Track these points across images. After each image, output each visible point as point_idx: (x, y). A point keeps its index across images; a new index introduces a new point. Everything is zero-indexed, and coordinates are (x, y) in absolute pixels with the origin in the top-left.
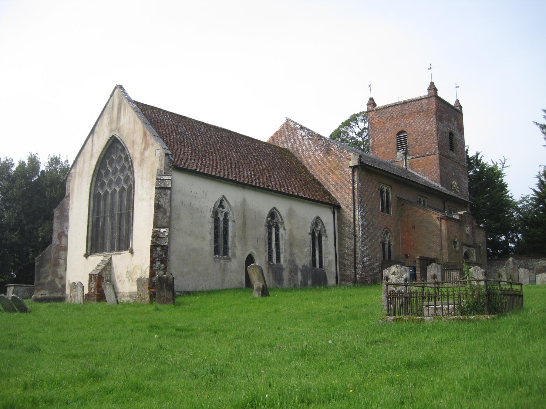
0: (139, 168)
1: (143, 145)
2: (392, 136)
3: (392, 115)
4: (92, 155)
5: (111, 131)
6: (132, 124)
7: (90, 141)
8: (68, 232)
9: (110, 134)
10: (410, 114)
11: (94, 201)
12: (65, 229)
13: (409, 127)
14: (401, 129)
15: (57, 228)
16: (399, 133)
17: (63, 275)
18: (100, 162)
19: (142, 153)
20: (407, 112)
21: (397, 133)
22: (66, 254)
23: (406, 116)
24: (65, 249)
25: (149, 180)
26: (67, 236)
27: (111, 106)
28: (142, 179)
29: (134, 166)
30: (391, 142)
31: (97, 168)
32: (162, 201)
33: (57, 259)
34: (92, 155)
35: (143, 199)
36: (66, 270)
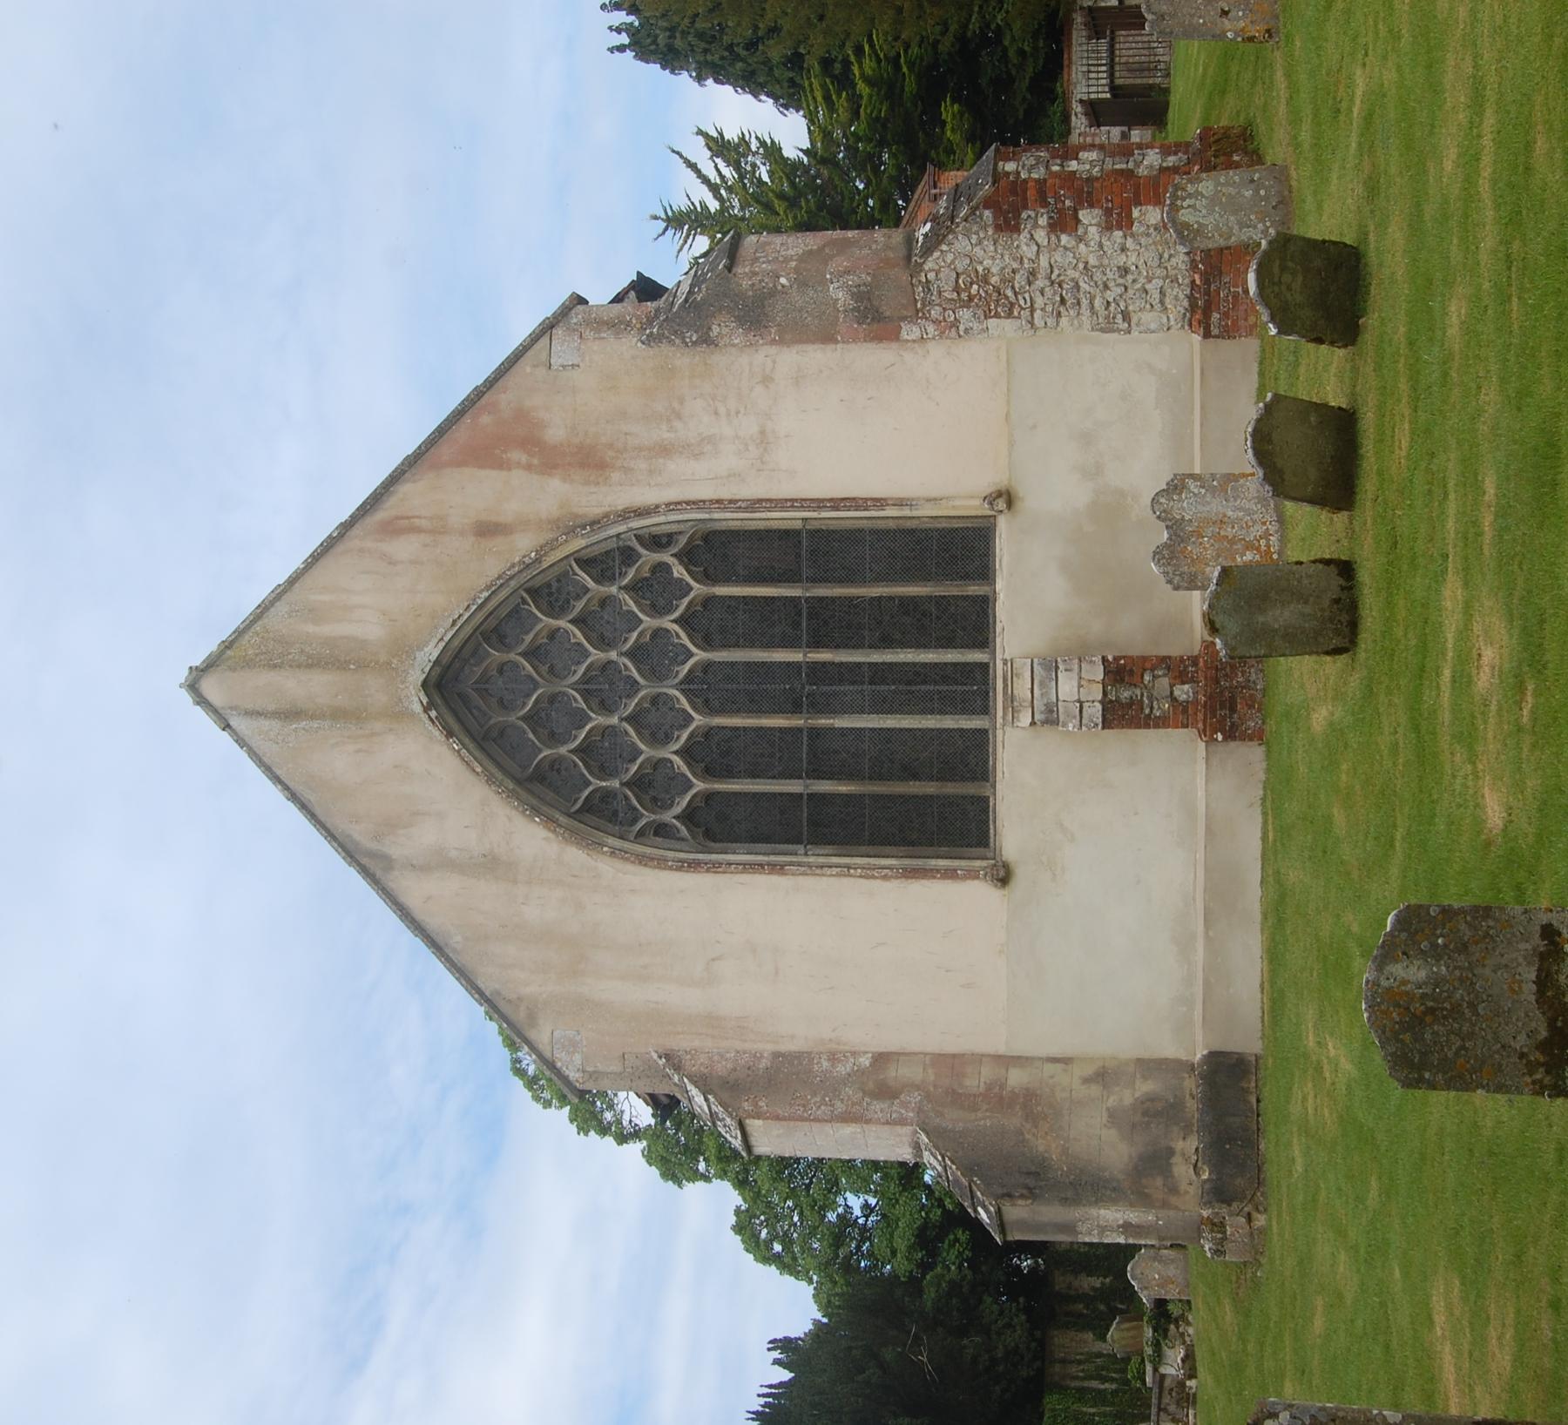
0: (616, 476)
1: (517, 455)
4: (491, 865)
5: (398, 714)
6: (404, 548)
7: (414, 890)
8: (854, 1054)
9: (413, 715)
11: (726, 853)
12: (842, 1069)
15: (838, 1104)
17: (1089, 1070)
18: (534, 802)
19: (550, 460)
22: (978, 1059)
24: (951, 1063)
25: (682, 401)
26: (881, 1059)
27: (273, 725)
28: (664, 450)
29: (596, 511)
31: (563, 819)
32: (791, 252)
33: (998, 1098)
34: (491, 865)
35: (763, 433)
36: (1065, 1061)
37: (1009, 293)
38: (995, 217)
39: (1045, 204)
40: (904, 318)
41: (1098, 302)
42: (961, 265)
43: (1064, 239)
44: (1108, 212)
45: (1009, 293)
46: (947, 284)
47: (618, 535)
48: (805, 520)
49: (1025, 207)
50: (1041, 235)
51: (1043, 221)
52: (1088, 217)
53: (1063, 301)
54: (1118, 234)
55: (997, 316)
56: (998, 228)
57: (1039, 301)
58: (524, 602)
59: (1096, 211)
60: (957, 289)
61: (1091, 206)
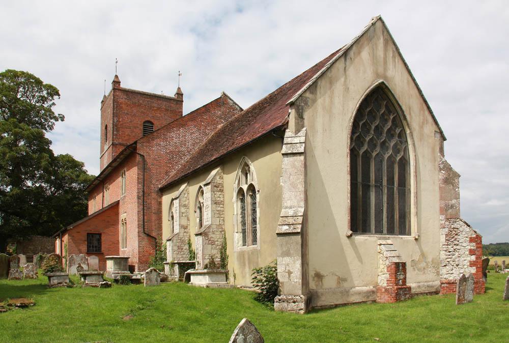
2: (139, 122)
3: (141, 102)
10: (158, 109)
13: (157, 120)
14: (149, 119)
16: (144, 122)
20: (156, 105)
21: (144, 120)
23: (155, 108)
30: (138, 127)
37: (452, 240)
38: (473, 238)
39: (477, 248)
40: (446, 216)
41: (449, 260)
42: (461, 229)
43: (468, 252)
44: (474, 262)
45: (452, 240)
46: (455, 225)
47: (407, 141)
48: (410, 189)
49: (476, 244)
50: (469, 247)
51: (472, 248)
52: (473, 258)
53: (450, 252)
54: (468, 264)
55: (446, 237)
56: (471, 238)
57: (450, 247)
58: (393, 114)
59: (475, 260)
60: (454, 228)
61: (476, 258)
